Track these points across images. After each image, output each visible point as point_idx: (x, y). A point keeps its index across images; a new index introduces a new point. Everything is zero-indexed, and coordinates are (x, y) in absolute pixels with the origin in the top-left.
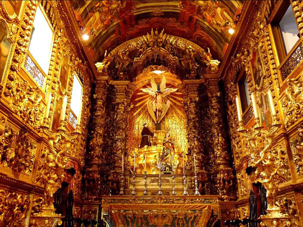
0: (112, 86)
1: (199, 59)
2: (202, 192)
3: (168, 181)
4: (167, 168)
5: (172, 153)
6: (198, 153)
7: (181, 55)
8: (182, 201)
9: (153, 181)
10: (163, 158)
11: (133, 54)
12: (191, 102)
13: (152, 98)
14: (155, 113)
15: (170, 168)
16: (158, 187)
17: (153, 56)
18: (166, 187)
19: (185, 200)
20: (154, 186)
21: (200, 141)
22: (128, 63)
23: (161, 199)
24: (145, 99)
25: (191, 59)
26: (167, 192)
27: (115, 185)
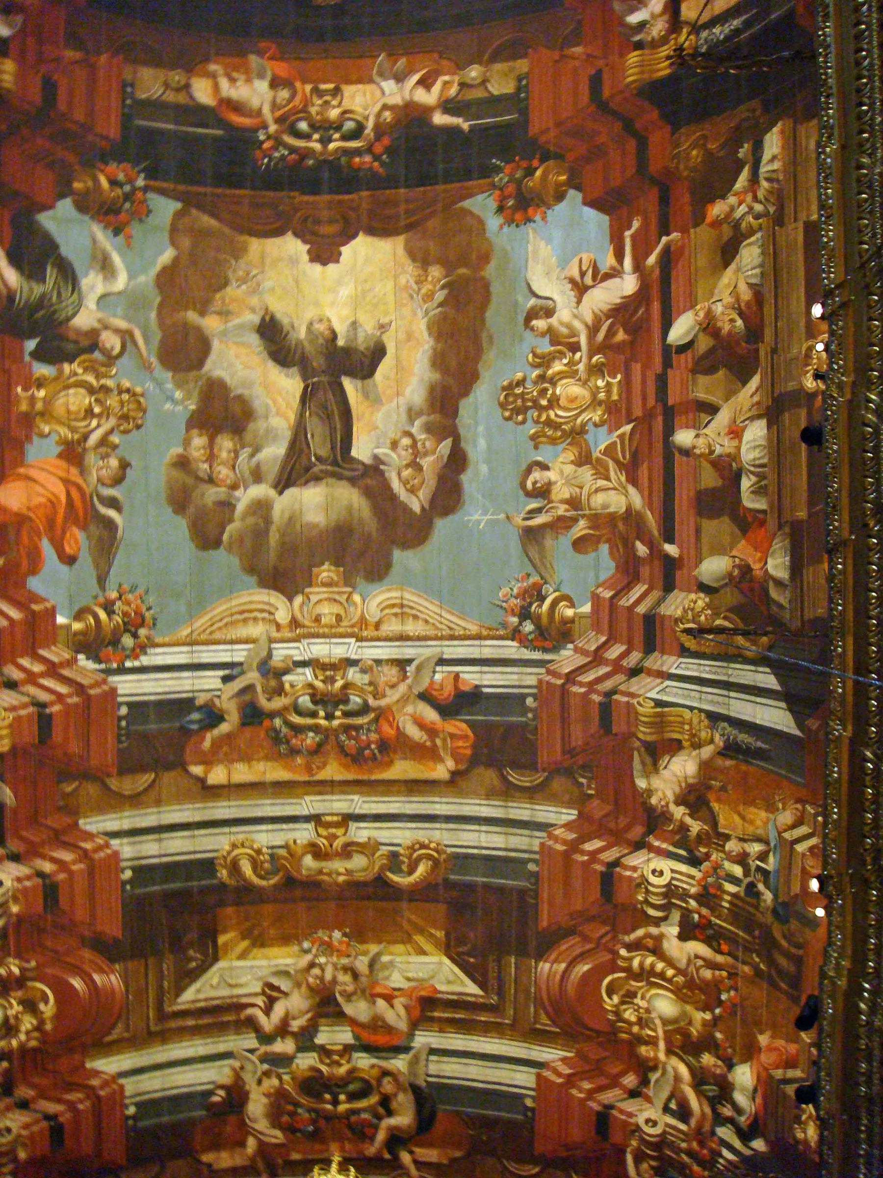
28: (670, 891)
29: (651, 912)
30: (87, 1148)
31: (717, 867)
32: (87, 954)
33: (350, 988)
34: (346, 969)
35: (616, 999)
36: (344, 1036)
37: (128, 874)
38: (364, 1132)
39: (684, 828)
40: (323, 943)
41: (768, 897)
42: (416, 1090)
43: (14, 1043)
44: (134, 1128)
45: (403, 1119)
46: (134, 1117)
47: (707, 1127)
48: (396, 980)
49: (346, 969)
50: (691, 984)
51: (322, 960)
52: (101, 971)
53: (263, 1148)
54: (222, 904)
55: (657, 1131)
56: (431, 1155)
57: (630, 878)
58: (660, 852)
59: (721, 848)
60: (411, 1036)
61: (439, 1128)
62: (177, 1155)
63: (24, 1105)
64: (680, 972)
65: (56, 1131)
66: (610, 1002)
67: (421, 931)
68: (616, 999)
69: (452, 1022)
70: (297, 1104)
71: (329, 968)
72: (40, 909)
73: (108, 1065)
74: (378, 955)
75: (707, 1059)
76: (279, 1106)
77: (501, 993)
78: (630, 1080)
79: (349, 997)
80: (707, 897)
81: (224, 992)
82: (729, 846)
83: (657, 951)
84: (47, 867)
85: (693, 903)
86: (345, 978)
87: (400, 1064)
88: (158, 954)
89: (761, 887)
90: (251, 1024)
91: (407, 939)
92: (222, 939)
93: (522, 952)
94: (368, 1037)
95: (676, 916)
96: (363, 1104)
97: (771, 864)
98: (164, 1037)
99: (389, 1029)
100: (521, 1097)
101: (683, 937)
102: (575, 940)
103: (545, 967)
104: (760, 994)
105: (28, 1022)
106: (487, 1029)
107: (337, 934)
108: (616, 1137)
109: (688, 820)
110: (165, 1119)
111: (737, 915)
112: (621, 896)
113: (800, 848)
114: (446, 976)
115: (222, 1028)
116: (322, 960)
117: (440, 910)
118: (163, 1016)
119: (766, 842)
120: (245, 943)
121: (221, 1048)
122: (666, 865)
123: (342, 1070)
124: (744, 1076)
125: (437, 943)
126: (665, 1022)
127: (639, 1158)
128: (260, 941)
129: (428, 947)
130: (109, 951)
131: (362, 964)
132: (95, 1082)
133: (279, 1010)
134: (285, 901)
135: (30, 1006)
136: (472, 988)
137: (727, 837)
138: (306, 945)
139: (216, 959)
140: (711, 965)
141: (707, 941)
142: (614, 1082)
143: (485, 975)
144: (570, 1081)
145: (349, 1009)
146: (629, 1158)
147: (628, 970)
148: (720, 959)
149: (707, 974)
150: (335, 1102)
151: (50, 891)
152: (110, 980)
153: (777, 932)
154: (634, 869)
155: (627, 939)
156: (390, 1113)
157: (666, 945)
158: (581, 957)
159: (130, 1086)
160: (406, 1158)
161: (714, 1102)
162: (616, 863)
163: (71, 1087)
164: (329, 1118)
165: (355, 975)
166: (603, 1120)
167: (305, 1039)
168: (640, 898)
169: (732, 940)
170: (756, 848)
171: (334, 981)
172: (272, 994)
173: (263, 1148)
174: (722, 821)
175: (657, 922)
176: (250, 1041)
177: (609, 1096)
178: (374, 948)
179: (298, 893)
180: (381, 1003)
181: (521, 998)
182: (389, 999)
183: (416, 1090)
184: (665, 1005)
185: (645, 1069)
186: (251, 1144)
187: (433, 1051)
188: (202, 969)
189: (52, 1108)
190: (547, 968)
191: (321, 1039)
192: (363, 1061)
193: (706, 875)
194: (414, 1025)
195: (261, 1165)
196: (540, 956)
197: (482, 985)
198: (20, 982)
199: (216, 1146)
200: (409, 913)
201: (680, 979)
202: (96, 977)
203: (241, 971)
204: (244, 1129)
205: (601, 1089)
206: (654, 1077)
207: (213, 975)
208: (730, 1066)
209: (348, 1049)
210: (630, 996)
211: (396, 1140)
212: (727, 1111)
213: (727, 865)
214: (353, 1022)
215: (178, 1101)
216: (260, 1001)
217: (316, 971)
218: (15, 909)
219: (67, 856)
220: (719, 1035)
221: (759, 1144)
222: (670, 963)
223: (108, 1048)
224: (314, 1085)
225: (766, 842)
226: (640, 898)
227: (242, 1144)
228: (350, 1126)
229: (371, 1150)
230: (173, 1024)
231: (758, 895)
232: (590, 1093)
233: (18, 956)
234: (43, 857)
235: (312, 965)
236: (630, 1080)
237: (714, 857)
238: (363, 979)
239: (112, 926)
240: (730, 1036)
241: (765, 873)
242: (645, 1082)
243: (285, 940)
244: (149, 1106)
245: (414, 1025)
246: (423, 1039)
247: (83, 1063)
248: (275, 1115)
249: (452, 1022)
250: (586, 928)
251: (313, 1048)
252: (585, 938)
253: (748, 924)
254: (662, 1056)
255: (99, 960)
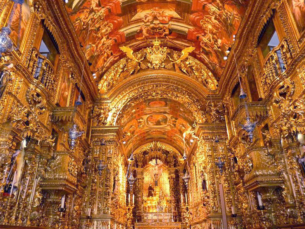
0: (135, 170)
1: (175, 157)
2: (176, 221)
3: (161, 215)
4: (161, 209)
5: (163, 202)
6: (174, 203)
7: (167, 154)
8: (167, 225)
9: (155, 215)
10: (159, 203)
11: (145, 153)
12: (172, 178)
13: (153, 166)
14: (155, 175)
15: (162, 209)
16: (157, 218)
17: (154, 155)
18: (160, 218)
19: (168, 224)
20: (155, 218)
21: (175, 198)
22: (143, 159)
23: (159, 224)
24: (149, 166)
25: (171, 157)
26: (161, 221)
27: (139, 217)
28: (214, 12)
29: (210, 14)
30: (120, 41)
31: (222, 12)
32: (116, 17)
33: (159, 15)
34: (158, 13)
35: (202, 23)
36: (158, 22)
37: (121, 4)
38: (161, 34)
39: (218, 4)
40: (154, 9)
41: (229, 21)
42: (169, 29)
43: (108, 32)
44: (127, 38)
45: (167, 32)
46: (126, 36)
47: (213, 44)
48: (167, 14)
49: (158, 13)
50: (215, 26)
51: (154, 12)
52: (119, 19)
53: (145, 37)
54: (137, 5)
55: (206, 41)
56: (171, 37)
57: (208, 8)
58: (213, 6)
59: (224, 10)
60: (169, 22)
61: (172, 34)
62: (132, 39)
63: (111, 39)
64: (213, 23)
65: (116, 41)
66: (201, 23)
67: (171, 8)
68: (202, 23)
69: (175, 21)
70: (150, 31)
71: (155, 13)
72: (108, 13)
73: (122, 30)
74: (163, 11)
75: (215, 36)
76: (148, 31)
77: (184, 18)
78: (203, 34)
79: (159, 17)
80: (219, 15)
81: (139, 17)
82: (226, 10)
83: (210, 19)
84: (108, 7)
85: (217, 15)
86: (158, 14)
87: (167, 26)
88: (127, 14)
89: (229, 19)
90: (143, 21)
91: (169, 9)
92: (137, 10)
93: (188, 13)
94: (161, 22)
95: (214, 16)
96: (161, 30)
97: (231, 17)
98: (129, 25)
99: (165, 21)
100: (185, 32)
101: (216, 19)
102: (197, 13)
103: (191, 16)
104: (225, 33)
105: (109, 29)
106: (181, 22)
107: (157, 8)
108: (199, 40)
109: (219, 3)
110: (131, 35)
111: (224, 20)
112: (206, 9)
113: (236, 19)
114: (175, 14)
115: (138, 22)
116: (154, 12)
117: (175, 5)
118: (129, 22)
119: (231, 14)
120: (141, 10)
121: (138, 25)
122: (214, 8)
123: (157, 27)
124: (220, 41)
125: (174, 10)
126: (209, 29)
127: (202, 43)
128: (144, 10)
129: (172, 10)
130: (120, 15)
131: (161, 12)
132: (120, 33)
133: (147, 19)
134: (148, 3)
135: (109, 27)
136: (179, 17)
137: (225, 9)
138: (152, 10)
139: (137, 13)
140: (218, 25)
141: (219, 22)
142: (200, 34)
143: (181, 15)
144: (193, 31)
145: (158, 18)
146: (201, 43)
147: (205, 20)
148: (220, 25)
149: (218, 26)
150: (156, 30)
151: (109, 10)
152: (121, 19)
153: (229, 27)
154: (209, 6)
155: (206, 16)
156: (165, 32)
157: (212, 19)
158: (198, 16)
159: (125, 32)
160: (167, 37)
161: (215, 41)
162: (206, 4)
163: (117, 35)
164: (156, 32)
165: (160, 14)
166: (198, 38)
167: (152, 23)
168: (209, 11)
169: (223, 24)
170: (229, 14)
171: (156, 14)
172: (146, 17)
173: (145, 37)
174: (225, 6)
175: (211, 15)
176: (143, 23)
177: (199, 35)
178: (163, 10)
179: (150, 2)
180: (164, 18)
181: (187, 19)
182: (165, 17)
183: (169, 29)
184: (210, 27)
185: (205, 34)
186: (144, 36)
187: (172, 24)
188: (135, 15)
189: (114, 38)
190: (192, 16)
191: (154, 23)
192: (161, 25)
193: (221, 13)
194: (169, 21)
195: (145, 38)
196: (191, 14)
197: (181, 16)
198: (107, 24)
199: (138, 37)
200: (169, 5)
201: (213, 24)
202: (118, 20)
203: (141, 14)
204: (142, 35)
205: (198, 34)
206: (206, 35)
207: (136, 15)
208: (218, 39)
209: (158, 24)
210: (205, 24)
211: (165, 35)
212: (216, 43)
213: (224, 13)
214: (159, 20)
215: (132, 33)
216: (144, 18)
217: (153, 13)
218: (104, 15)
219: (111, 4)
220: (217, 34)
221: (220, 50)
222: (212, 22)
223: (120, 28)
224: (153, 28)
225: (231, 14)
226: (209, 11)
227: (142, 36)
228: (159, 33)
229: (162, 36)
230: (131, 23)
231: (228, 20)
232: (196, 34)
233: (106, 21)
234: (107, 6)
235: (153, 12)
236: (203, 34)
237: (222, 11)
238: (161, 14)
239: (120, 12)
240: (219, 35)
241: (230, 18)
242: (205, 35)
243: (148, 9)
244: (128, 34)
245: (169, 21)
246: (170, 23)
247: (118, 32)
248: (147, 33)
249: (175, 21)
250: (199, 12)
251: (153, 24)
252: (199, 14)
253: (226, 23)
254: (208, 33)
255: (119, 17)
